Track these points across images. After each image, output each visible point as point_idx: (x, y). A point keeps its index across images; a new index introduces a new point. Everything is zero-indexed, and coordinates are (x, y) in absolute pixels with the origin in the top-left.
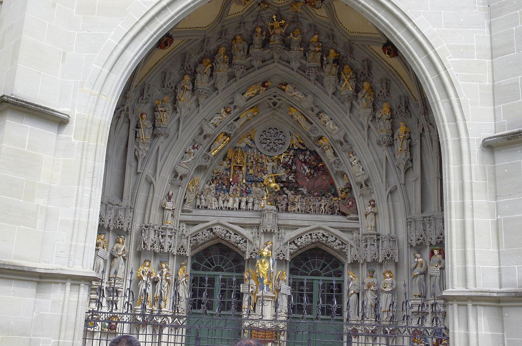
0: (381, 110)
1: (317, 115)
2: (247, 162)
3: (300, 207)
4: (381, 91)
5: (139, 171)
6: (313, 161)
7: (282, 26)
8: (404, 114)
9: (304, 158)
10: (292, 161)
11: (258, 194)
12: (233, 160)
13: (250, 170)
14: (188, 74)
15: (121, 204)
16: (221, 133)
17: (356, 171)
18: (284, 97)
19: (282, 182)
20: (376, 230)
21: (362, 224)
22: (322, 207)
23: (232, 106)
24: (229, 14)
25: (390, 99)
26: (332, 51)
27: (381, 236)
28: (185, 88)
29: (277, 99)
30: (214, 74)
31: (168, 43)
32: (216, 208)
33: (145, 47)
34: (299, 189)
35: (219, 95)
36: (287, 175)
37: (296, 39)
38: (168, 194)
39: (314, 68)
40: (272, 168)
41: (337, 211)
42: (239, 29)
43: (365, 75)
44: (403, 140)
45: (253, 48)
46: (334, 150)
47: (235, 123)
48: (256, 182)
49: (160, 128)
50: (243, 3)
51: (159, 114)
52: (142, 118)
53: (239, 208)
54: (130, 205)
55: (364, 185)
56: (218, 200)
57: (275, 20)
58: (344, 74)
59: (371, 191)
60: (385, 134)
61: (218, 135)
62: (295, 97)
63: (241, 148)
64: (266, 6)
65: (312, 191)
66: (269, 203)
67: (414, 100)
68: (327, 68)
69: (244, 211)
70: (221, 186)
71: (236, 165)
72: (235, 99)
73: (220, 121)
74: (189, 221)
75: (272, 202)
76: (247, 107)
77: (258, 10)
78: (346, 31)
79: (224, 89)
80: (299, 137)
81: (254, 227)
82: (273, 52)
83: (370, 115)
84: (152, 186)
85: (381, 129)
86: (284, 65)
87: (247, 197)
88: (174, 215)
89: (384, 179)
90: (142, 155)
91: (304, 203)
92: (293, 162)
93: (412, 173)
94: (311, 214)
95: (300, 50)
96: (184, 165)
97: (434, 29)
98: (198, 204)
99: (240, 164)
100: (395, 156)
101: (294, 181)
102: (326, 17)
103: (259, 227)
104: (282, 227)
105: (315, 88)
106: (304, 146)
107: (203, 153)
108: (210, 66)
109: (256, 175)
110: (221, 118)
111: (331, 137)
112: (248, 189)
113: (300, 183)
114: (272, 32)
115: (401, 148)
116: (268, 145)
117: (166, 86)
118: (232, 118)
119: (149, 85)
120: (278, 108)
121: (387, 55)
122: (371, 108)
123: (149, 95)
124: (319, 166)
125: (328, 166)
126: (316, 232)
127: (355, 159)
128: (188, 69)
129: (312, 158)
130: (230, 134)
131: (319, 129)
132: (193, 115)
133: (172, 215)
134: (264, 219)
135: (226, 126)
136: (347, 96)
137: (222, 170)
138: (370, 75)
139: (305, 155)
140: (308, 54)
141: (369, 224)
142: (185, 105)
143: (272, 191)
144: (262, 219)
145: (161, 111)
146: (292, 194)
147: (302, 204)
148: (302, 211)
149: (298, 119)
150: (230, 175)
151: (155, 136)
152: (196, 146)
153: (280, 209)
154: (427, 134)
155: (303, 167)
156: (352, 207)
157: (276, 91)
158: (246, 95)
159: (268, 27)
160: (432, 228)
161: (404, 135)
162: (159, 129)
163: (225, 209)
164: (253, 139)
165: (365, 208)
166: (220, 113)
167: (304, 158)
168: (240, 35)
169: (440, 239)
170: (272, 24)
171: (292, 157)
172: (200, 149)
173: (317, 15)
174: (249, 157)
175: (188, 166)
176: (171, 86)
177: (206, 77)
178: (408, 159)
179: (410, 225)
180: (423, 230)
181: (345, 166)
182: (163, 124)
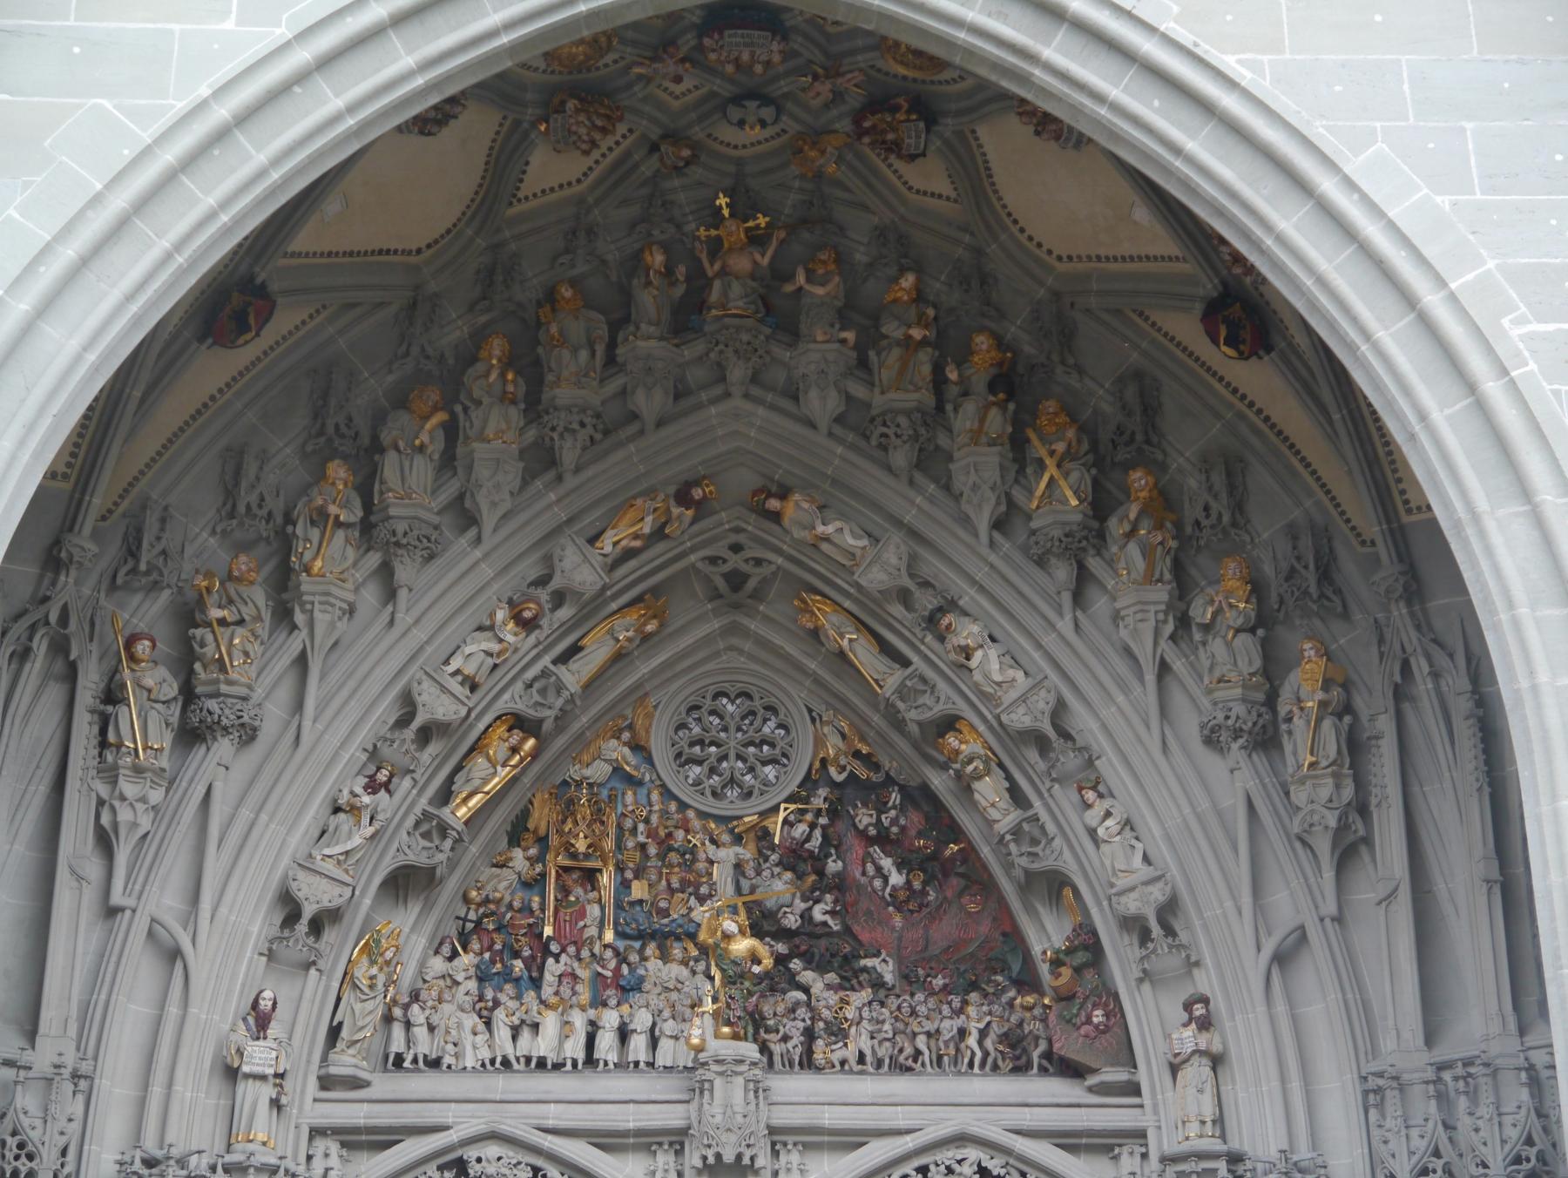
0: (1210, 590)
1: (932, 621)
3: (869, 1043)
4: (1207, 508)
5: (117, 898)
6: (920, 835)
7: (756, 239)
8: (1314, 602)
9: (879, 820)
10: (825, 836)
11: (674, 996)
12: (554, 840)
13: (636, 885)
14: (345, 458)
15: (27, 1057)
16: (499, 718)
17: (1118, 866)
18: (779, 552)
19: (784, 934)
20: (1223, 1137)
21: (1156, 1112)
22: (972, 1041)
23: (544, 595)
24: (521, 195)
25: (1248, 539)
26: (982, 341)
27: (1249, 1165)
28: (328, 516)
29: (747, 561)
30: (460, 450)
31: (252, 321)
32: (483, 1065)
33: (134, 308)
34: (863, 962)
35: (487, 545)
36: (804, 899)
37: (820, 291)
38: (255, 1005)
39: (908, 413)
40: (731, 871)
41: (1042, 1056)
42: (569, 257)
43: (1132, 440)
44: (1319, 721)
45: (631, 338)
46: (1009, 777)
47: (562, 671)
48: (663, 939)
49: (214, 701)
50: (584, 142)
51: (209, 638)
52: (132, 658)
53: (590, 1061)
54: (70, 1059)
55: (1156, 930)
56: (488, 1024)
57: (726, 212)
58: (1041, 439)
59: (1188, 957)
60: (1238, 692)
61: (481, 726)
62: (825, 547)
63: (591, 785)
64: (686, 153)
65: (921, 972)
66: (726, 1030)
67: (1354, 542)
68: (964, 418)
69: (609, 1071)
70: (502, 961)
71: (568, 863)
72: (556, 561)
73: (490, 661)
74: (356, 1130)
75: (742, 1023)
76: (615, 597)
77: (648, 174)
78: (1042, 254)
79: (505, 517)
80: (852, 725)
81: (660, 1144)
82: (721, 352)
83: (1166, 613)
84: (179, 965)
85: (1217, 674)
86: (773, 407)
87: (625, 1008)
88: (284, 1100)
89: (1246, 900)
90: (135, 825)
91: (887, 1027)
93: (1370, 867)
94: (920, 1074)
95: (843, 341)
96: (329, 867)
97: (1439, 199)
98: (397, 1045)
99: (587, 856)
100: (1287, 794)
101: (835, 925)
102: (948, 199)
103: (682, 1144)
104: (790, 1139)
105: (916, 505)
107: (418, 810)
108: (440, 417)
109: (663, 904)
110: (495, 647)
111: (998, 718)
112: (625, 969)
113: (865, 937)
114: (717, 266)
115: (1312, 754)
117: (242, 509)
118: (546, 650)
119: (166, 508)
120: (749, 601)
121: (1224, 348)
122: (1169, 583)
123: (164, 552)
124: (948, 853)
125: (986, 852)
126: (948, 1156)
127: (1108, 814)
128: (343, 436)
129: (914, 820)
130: (541, 721)
131: (942, 685)
132: (370, 635)
133: (276, 1104)
134: (706, 1107)
135: (519, 685)
136: (1057, 533)
137: (507, 888)
138: (1155, 439)
139: (881, 808)
140: (878, 354)
141: (1192, 1110)
142: (328, 594)
143: (735, 975)
144: (694, 1106)
145: (222, 622)
146: (829, 987)
147: (880, 1031)
148: (879, 1064)
149: (845, 643)
150: (543, 910)
151: (191, 735)
152: (382, 776)
153: (777, 1059)
154: (1423, 685)
155: (874, 862)
156: (1104, 1032)
157: (744, 526)
158: (607, 544)
159: (697, 244)
160: (1485, 1111)
161: (1320, 695)
162: (212, 704)
163: (522, 1067)
165: (1167, 1036)
166: (491, 628)
167: (879, 820)
168: (573, 283)
169: (1525, 1166)
170: (713, 232)
172: (398, 796)
173: (910, 188)
174: (628, 824)
175: (347, 871)
176: (264, 512)
177: (421, 471)
178: (1349, 804)
179: (1380, 1106)
180: (1440, 1128)
181: (1065, 849)
182: (230, 683)
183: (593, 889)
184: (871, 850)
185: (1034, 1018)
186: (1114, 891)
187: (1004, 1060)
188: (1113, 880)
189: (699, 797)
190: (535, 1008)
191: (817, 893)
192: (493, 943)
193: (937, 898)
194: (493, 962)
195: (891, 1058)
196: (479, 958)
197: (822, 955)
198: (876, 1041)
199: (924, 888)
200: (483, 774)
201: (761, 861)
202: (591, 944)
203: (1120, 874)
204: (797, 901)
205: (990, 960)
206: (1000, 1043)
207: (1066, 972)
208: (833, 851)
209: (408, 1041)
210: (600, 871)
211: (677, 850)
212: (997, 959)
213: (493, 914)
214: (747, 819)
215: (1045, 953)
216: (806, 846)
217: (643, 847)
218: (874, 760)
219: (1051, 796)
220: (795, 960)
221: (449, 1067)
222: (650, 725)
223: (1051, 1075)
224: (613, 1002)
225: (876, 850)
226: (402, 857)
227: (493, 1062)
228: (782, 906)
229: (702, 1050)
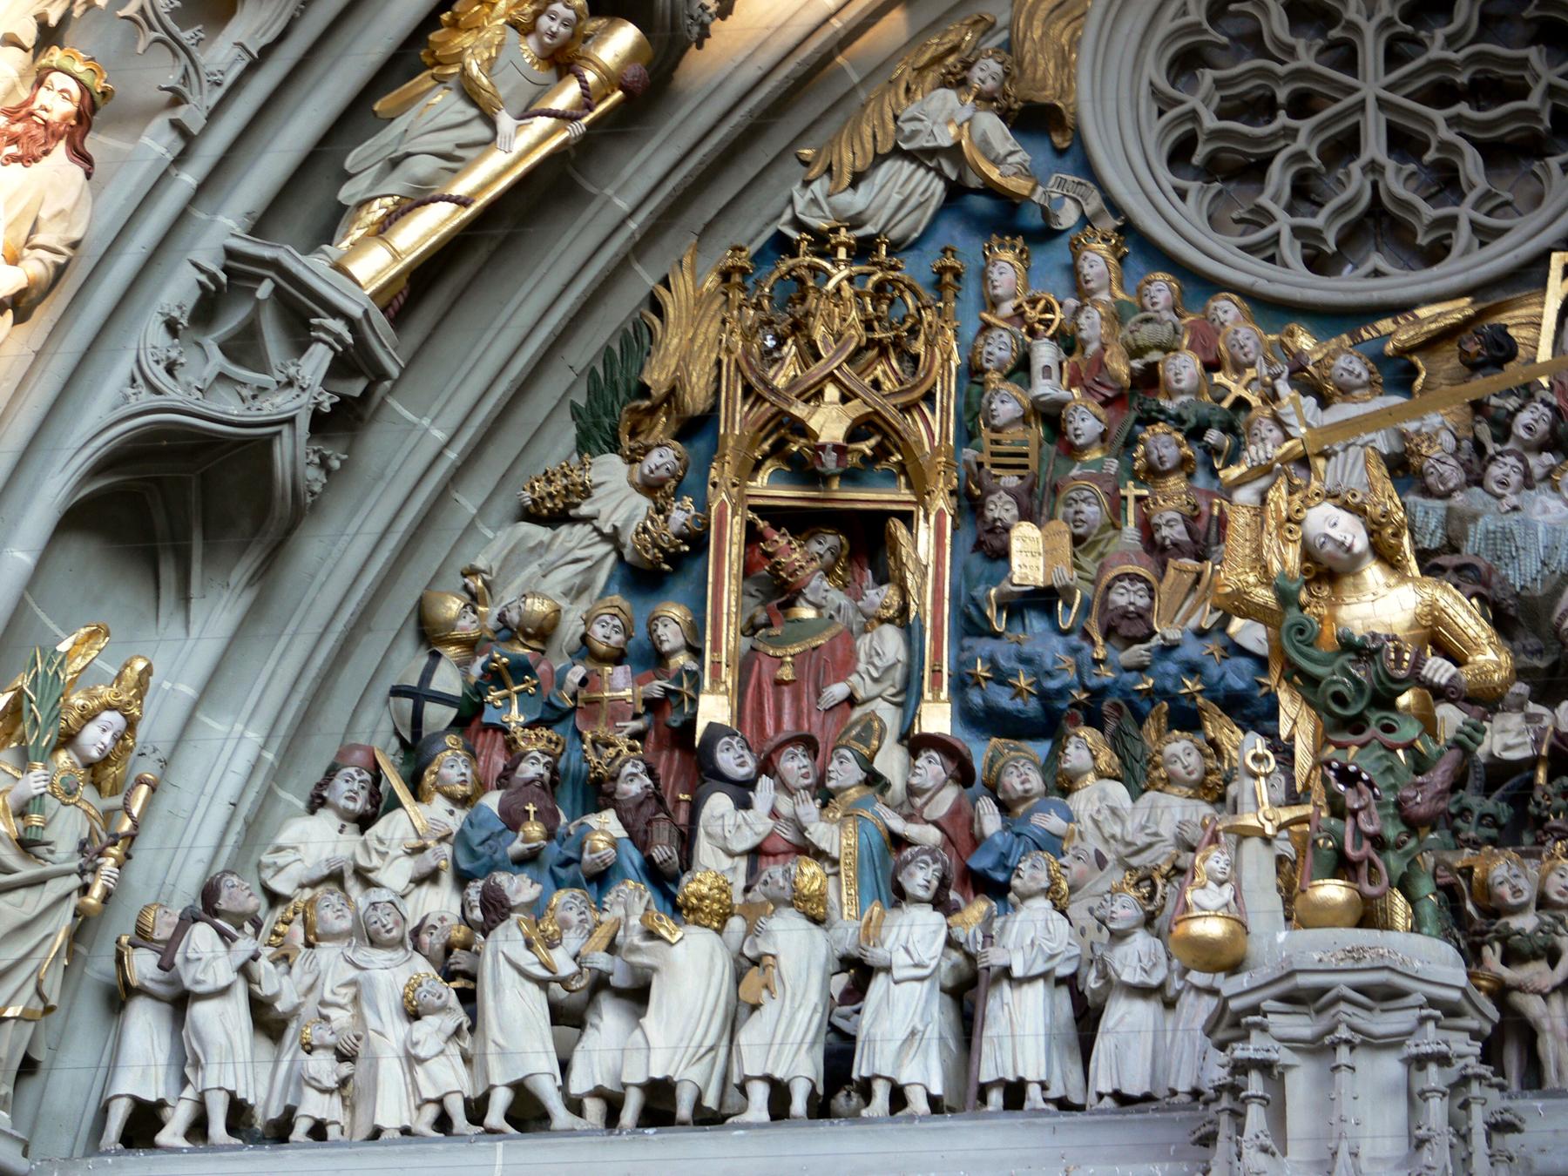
2: (967, 435)
12: (737, 419)
32: (443, 1123)
56: (468, 998)
63: (863, 250)
70: (548, 818)
71: (787, 494)
75: (1394, 863)
109: (1126, 597)
112: (990, 821)
116: (1304, 192)
137: (576, 592)
150: (696, 652)
164: (1047, 96)
174: (1000, 348)
183: (881, 580)
189: (1256, 264)
190: (635, 921)
192: (515, 756)
194: (512, 820)
196: (461, 814)
200: (446, 141)
201: (1484, 432)
202: (863, 739)
209: (185, 1062)
210: (907, 518)
211: (1178, 420)
213: (520, 670)
214: (1423, 312)
217: (1051, 417)
221: (318, 1131)
222: (1075, 43)
224: (920, 879)
226: (146, 399)
227: (476, 1110)
229: (1234, 968)
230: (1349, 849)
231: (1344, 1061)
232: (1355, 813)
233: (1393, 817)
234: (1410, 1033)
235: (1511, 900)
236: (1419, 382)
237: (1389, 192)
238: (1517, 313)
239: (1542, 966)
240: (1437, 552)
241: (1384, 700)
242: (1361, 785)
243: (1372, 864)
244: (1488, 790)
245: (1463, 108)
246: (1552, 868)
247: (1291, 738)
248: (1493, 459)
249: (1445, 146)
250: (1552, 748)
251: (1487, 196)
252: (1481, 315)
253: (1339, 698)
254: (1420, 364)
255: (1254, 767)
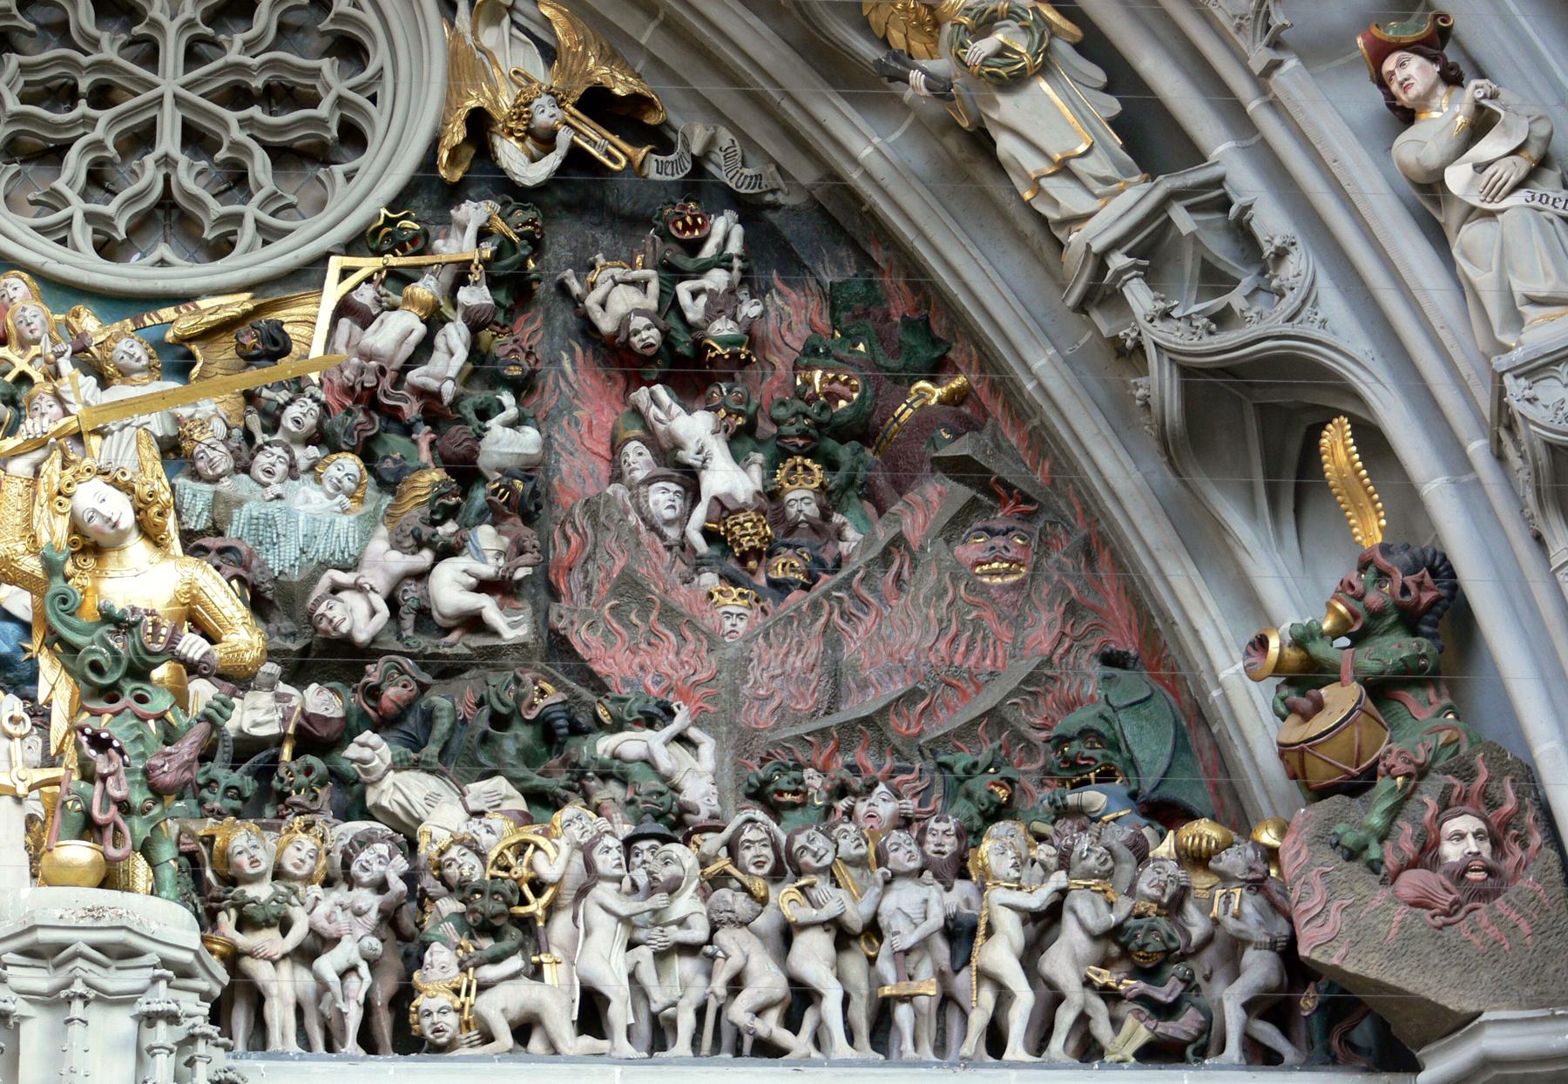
9: (670, 306)
17: (1519, 287)
75: (138, 828)
91: (686, 904)
92: (481, 367)
94: (806, 1061)
106: (661, 140)
116: (98, 179)
124: (905, 412)
127: (1481, 123)
153: (280, 1015)
156: (1484, 895)
167: (670, 306)
171: (475, 296)
184: (641, 395)
185: (1225, 878)
186: (1517, 356)
187: (1116, 1023)
188: (1507, 339)
189: (47, 245)
191: (450, 527)
193: (869, 542)
195: (701, 1012)
197: (459, 724)
198: (644, 954)
199: (825, 516)
201: (255, 422)
203: (1531, 312)
204: (379, 544)
205: (1062, 740)
206: (1105, 963)
207: (1341, 698)
208: (507, 398)
212: (1085, 733)
214: (204, 303)
215: (1261, 643)
216: (414, 376)
218: (652, 120)
219: (1274, 105)
220: (368, 736)
223: (1291, 1068)
225: (658, 402)
228: (324, 566)
230: (96, 812)
231: (78, 1016)
232: (104, 778)
233: (141, 783)
234: (143, 992)
235: (249, 870)
236: (195, 371)
237: (179, 184)
238: (293, 311)
239: (274, 933)
240: (202, 533)
241: (139, 672)
242: (112, 752)
243: (117, 828)
244: (236, 761)
245: (256, 112)
246: (290, 841)
247: (49, 703)
248: (261, 448)
249: (235, 146)
250: (299, 727)
251: (273, 197)
252: (258, 310)
253: (96, 667)
254: (198, 353)
255: (10, 728)
